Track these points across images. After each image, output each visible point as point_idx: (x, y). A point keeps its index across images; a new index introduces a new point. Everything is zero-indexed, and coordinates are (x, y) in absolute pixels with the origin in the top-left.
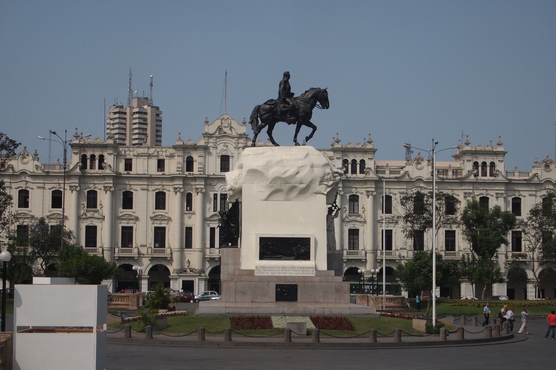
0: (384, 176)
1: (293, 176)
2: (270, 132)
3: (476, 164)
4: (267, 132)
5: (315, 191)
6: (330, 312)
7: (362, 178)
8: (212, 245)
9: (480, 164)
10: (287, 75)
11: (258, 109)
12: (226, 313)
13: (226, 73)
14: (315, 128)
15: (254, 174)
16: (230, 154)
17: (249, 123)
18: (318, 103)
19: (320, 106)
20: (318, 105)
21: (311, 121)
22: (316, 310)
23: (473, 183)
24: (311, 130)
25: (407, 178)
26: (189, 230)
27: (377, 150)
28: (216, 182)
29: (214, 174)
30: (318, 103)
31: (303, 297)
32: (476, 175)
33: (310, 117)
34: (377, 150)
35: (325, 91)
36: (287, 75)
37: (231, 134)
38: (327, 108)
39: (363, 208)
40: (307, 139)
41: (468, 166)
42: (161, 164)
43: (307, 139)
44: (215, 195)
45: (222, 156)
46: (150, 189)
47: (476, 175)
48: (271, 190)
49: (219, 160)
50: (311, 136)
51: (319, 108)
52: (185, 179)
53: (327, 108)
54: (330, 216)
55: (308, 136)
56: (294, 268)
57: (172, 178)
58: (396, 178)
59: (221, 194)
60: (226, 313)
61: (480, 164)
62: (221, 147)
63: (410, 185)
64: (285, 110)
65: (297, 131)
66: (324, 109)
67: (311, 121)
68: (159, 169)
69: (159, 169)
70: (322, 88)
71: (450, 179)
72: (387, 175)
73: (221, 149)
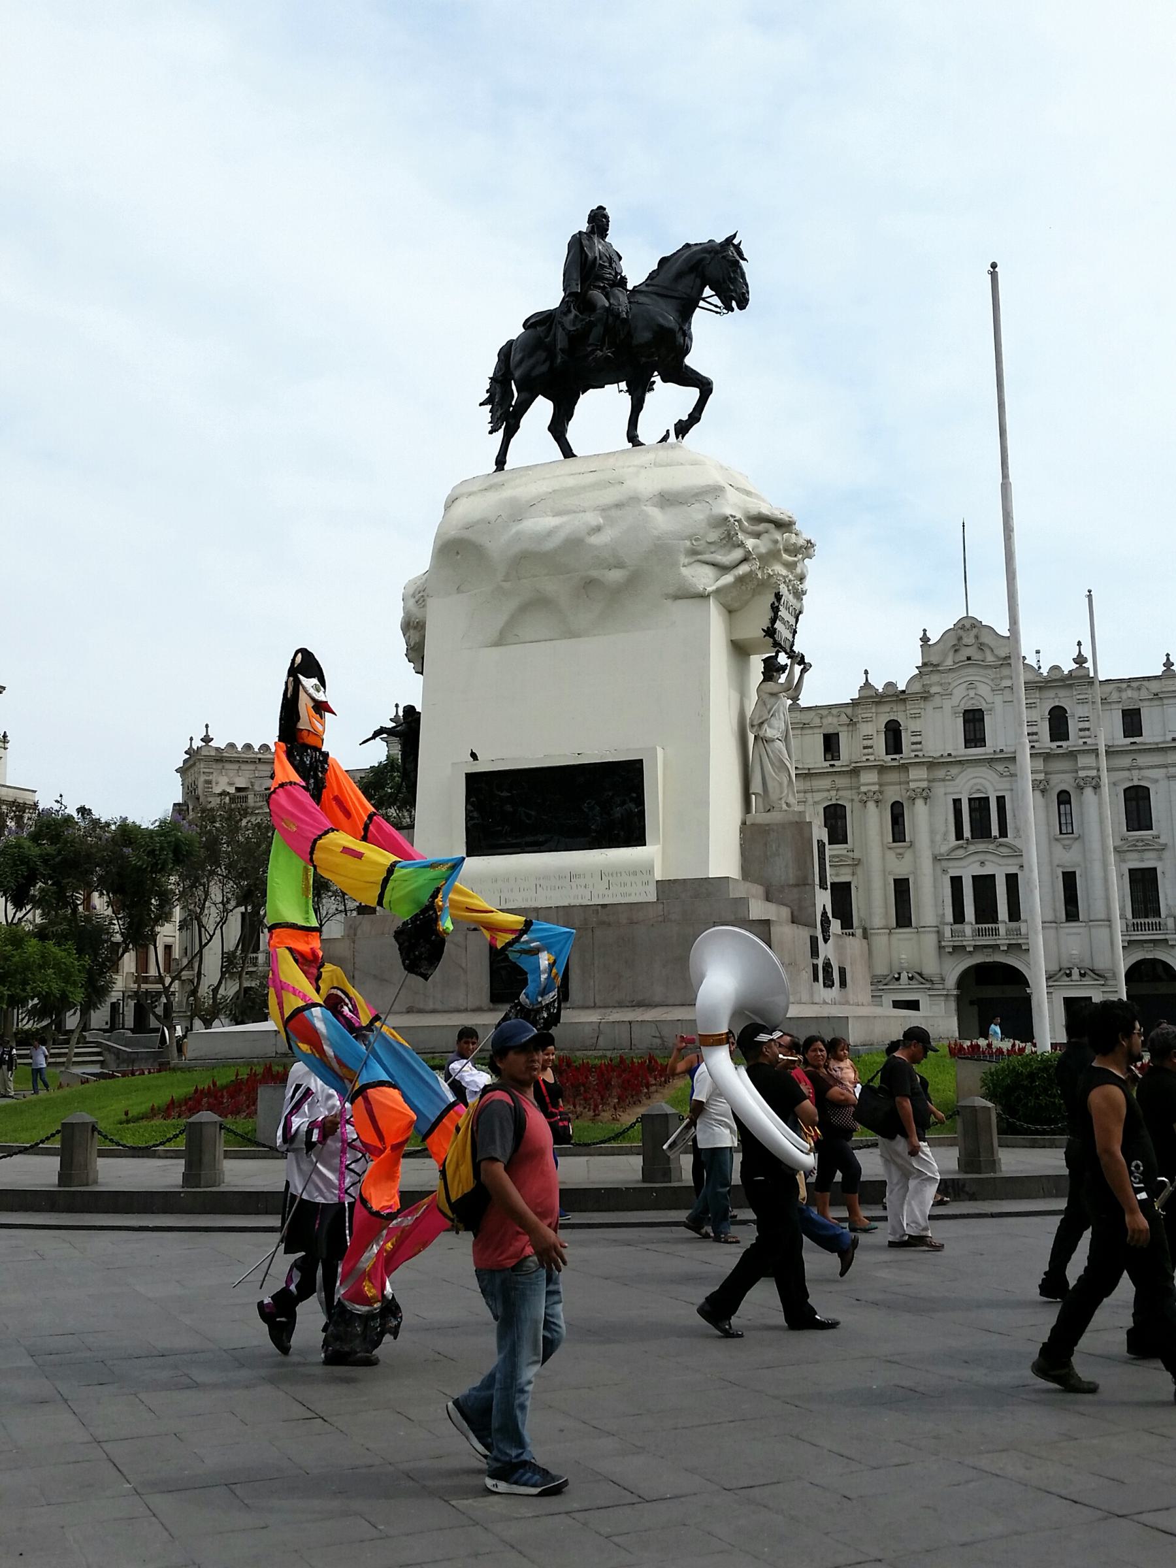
1: (574, 544)
2: (558, 428)
4: (550, 429)
5: (671, 590)
6: (658, 1041)
8: (959, 917)
10: (599, 221)
12: (277, 1053)
13: (964, 526)
14: (705, 388)
15: (459, 557)
16: (984, 706)
18: (708, 291)
19: (716, 300)
21: (689, 361)
22: (600, 1032)
24: (694, 393)
26: (902, 888)
28: (954, 770)
29: (949, 755)
30: (708, 291)
31: (592, 983)
33: (686, 350)
36: (599, 221)
37: (983, 661)
40: (682, 428)
42: (831, 744)
43: (682, 428)
44: (957, 803)
45: (966, 712)
46: (810, 801)
48: (512, 605)
49: (961, 720)
50: (695, 416)
51: (717, 313)
52: (882, 769)
55: (685, 418)
56: (577, 876)
57: (855, 772)
59: (970, 800)
60: (277, 1053)
62: (959, 692)
64: (577, 329)
65: (637, 407)
66: (732, 310)
67: (689, 361)
68: (829, 756)
69: (829, 756)
73: (960, 697)
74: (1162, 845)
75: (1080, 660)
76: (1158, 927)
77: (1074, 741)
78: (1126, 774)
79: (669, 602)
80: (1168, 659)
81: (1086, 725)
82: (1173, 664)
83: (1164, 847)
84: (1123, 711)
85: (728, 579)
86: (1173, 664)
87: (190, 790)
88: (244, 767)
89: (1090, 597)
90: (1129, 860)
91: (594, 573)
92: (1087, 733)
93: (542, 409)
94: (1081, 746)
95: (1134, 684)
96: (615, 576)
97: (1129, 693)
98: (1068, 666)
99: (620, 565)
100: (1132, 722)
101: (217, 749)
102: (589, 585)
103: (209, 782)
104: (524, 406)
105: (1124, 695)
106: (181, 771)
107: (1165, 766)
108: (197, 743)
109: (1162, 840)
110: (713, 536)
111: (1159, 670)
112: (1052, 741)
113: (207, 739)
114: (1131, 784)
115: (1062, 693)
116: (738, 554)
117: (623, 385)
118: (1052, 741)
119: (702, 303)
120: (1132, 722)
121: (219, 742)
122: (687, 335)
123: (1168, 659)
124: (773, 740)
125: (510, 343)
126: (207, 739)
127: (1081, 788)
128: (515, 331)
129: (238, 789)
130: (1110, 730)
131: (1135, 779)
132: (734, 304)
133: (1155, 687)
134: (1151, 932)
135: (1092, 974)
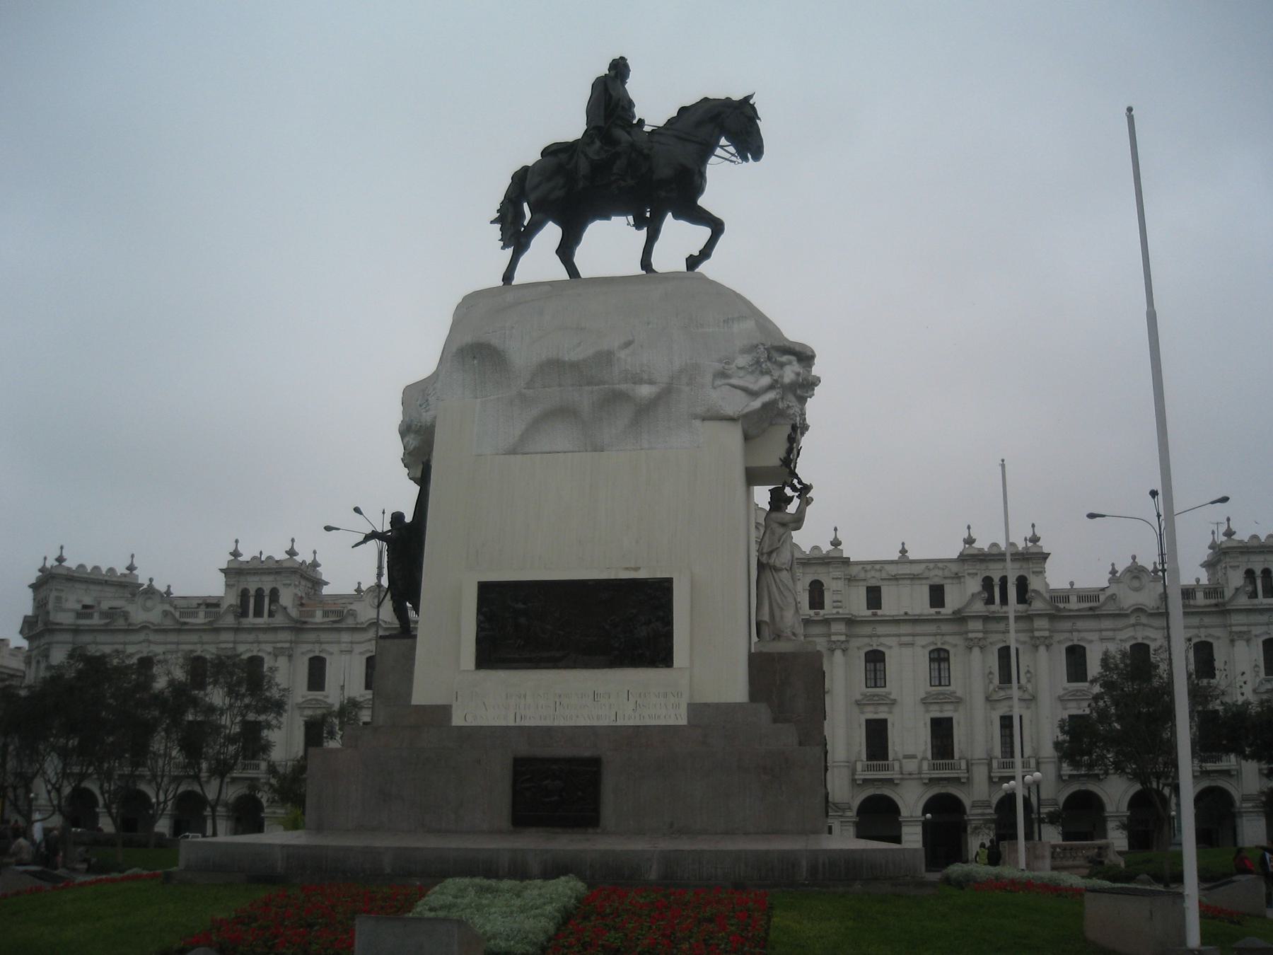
0: (1067, 606)
2: (566, 251)
3: (1250, 574)
4: (557, 252)
5: (700, 410)
7: (1022, 613)
9: (1258, 573)
11: (521, 179)
14: (717, 227)
17: (492, 222)
18: (723, 141)
20: (722, 147)
21: (703, 201)
23: (1249, 611)
24: (705, 232)
25: (1110, 608)
27: (1049, 554)
30: (723, 141)
32: (1254, 595)
33: (699, 190)
34: (1049, 554)
35: (747, 99)
38: (758, 154)
39: (1028, 672)
40: (693, 262)
41: (1236, 579)
47: (1254, 595)
50: (706, 253)
53: (758, 154)
54: (774, 515)
55: (697, 253)
58: (1091, 609)
61: (1258, 573)
63: (1120, 623)
67: (703, 201)
70: (737, 96)
71: (1199, 607)
72: (1074, 604)
74: (892, 700)
75: (836, 543)
76: (887, 768)
77: (829, 610)
78: (867, 640)
79: (697, 423)
80: (903, 547)
81: (839, 598)
82: (907, 552)
83: (894, 702)
84: (867, 588)
85: (757, 404)
86: (907, 552)
87: (40, 604)
88: (92, 587)
89: (1003, 466)
90: (931, 711)
91: (623, 387)
92: (839, 604)
93: (551, 233)
94: (834, 614)
95: (878, 567)
96: (645, 391)
97: (873, 573)
98: (826, 547)
99: (651, 382)
100: (874, 597)
101: (69, 569)
102: (615, 398)
103: (58, 599)
104: (535, 227)
105: (869, 575)
106: (35, 587)
107: (899, 636)
108: (51, 562)
109: (892, 697)
110: (743, 360)
111: (895, 556)
112: (811, 608)
113: (60, 559)
114: (871, 649)
115: (821, 569)
116: (765, 381)
117: (631, 218)
118: (811, 608)
119: (718, 151)
120: (874, 597)
121: (71, 563)
122: (702, 176)
123: (903, 547)
124: (781, 570)
125: (525, 169)
126: (60, 559)
127: (832, 651)
128: (532, 156)
129: (85, 607)
130: (857, 604)
131: (875, 645)
132: (749, 156)
133: (893, 570)
134: (872, 773)
135: (834, 807)
